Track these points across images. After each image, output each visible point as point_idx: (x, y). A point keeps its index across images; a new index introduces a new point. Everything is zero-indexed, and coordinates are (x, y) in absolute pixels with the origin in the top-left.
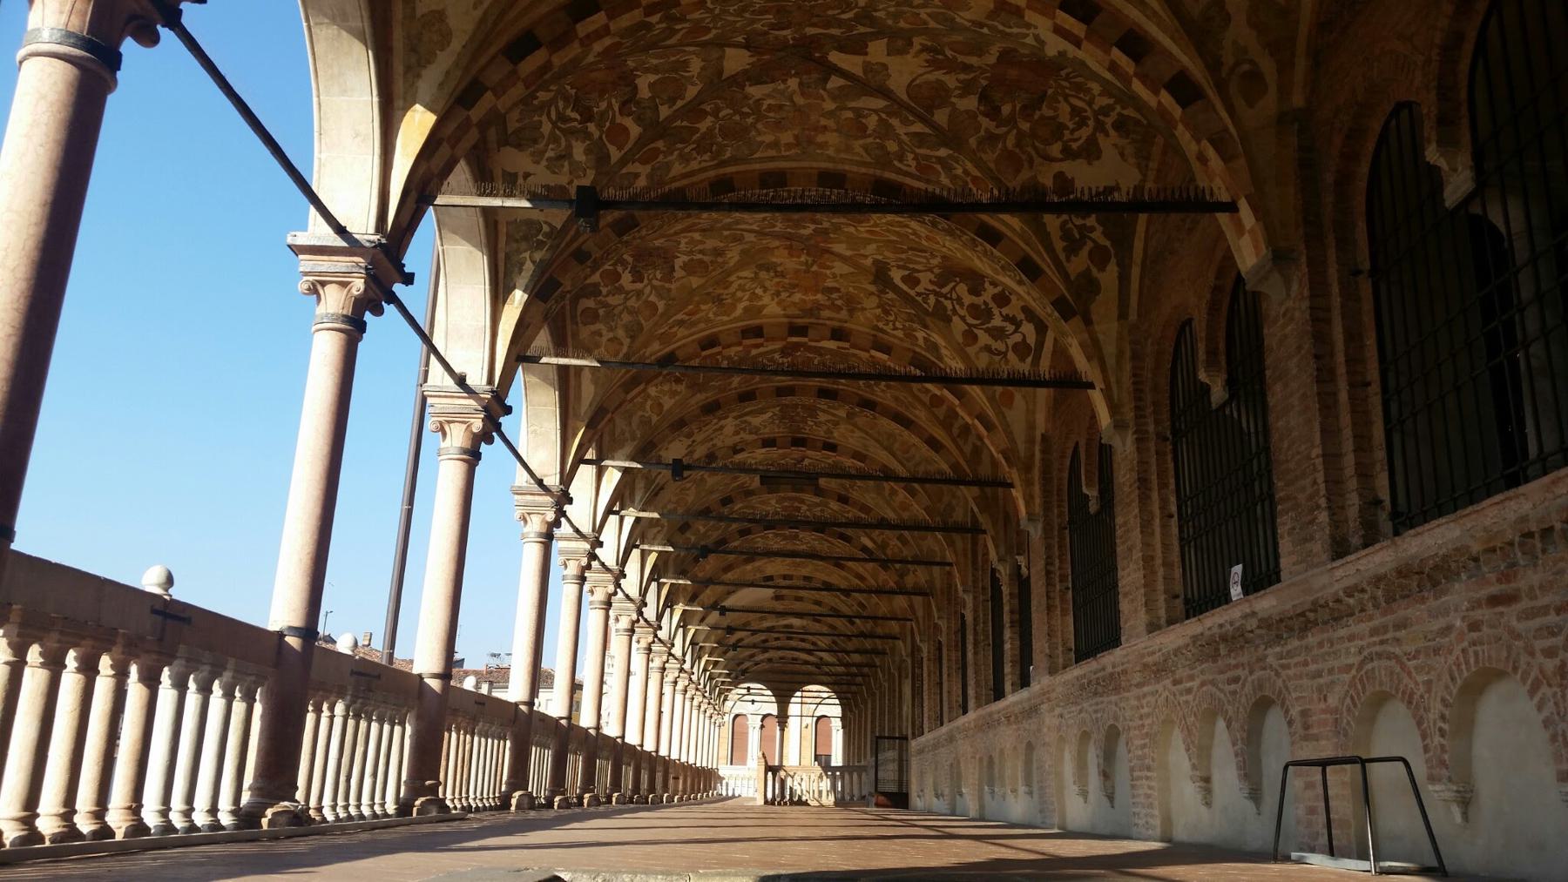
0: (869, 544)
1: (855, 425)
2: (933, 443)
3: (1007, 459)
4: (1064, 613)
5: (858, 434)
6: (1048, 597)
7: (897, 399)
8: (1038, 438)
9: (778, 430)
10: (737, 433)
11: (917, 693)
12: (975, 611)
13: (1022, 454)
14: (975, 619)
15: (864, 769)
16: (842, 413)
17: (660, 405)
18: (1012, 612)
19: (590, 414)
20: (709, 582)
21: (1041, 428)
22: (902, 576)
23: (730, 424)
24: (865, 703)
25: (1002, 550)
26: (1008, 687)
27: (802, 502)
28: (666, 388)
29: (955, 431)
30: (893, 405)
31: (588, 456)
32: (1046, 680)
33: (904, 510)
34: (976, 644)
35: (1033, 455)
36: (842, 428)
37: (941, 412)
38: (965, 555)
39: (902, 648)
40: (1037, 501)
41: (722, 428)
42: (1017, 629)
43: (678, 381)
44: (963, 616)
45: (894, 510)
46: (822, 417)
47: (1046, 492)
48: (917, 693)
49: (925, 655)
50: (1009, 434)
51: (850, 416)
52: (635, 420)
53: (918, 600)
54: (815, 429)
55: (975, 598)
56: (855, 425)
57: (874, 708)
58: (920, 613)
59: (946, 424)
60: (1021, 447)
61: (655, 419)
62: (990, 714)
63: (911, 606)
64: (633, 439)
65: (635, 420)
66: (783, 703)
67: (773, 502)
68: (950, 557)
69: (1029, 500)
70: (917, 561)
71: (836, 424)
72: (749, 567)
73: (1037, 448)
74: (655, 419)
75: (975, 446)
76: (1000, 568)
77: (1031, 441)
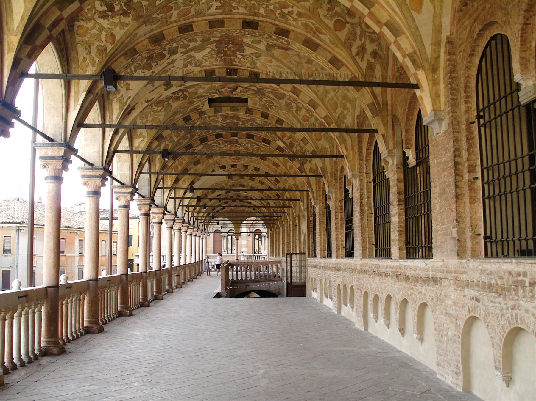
0: (282, 145)
1: (272, 56)
2: (335, 62)
3: (414, 62)
4: (473, 200)
5: (275, 63)
6: (456, 186)
7: (306, 26)
8: (444, 41)
9: (216, 65)
10: (186, 66)
11: (312, 230)
12: (361, 189)
13: (429, 57)
14: (361, 195)
15: (279, 262)
16: (262, 47)
17: (113, 36)
18: (399, 193)
19: (22, 28)
20: (185, 172)
21: (446, 32)
22: (302, 164)
23: (179, 58)
24: (279, 228)
25: (391, 145)
26: (395, 250)
27: (239, 119)
28: (116, 20)
29: (354, 51)
30: (303, 32)
31: (30, 72)
32: (453, 262)
33: (306, 121)
34: (362, 212)
35: (439, 56)
36: (263, 59)
37: (343, 34)
38: (353, 150)
39: (303, 205)
40: (443, 99)
41: (173, 62)
42: (403, 206)
43: (125, 14)
44: (346, 191)
45: (299, 121)
46: (248, 51)
47: (453, 91)
48: (312, 230)
49: (317, 211)
50: (417, 37)
51: (269, 47)
52: (94, 50)
53: (313, 180)
54: (243, 63)
55: (361, 180)
56: (272, 56)
57: (283, 232)
58: (314, 187)
59: (347, 45)
60: (429, 49)
61: (109, 47)
62: (378, 267)
63: (309, 183)
64: (93, 65)
65: (94, 50)
66: (238, 225)
67: (220, 120)
68: (344, 152)
69: (435, 97)
70: (314, 155)
71: (258, 56)
72: (211, 161)
73: (442, 50)
74: (109, 47)
75: (369, 61)
76: (390, 160)
77: (437, 44)
